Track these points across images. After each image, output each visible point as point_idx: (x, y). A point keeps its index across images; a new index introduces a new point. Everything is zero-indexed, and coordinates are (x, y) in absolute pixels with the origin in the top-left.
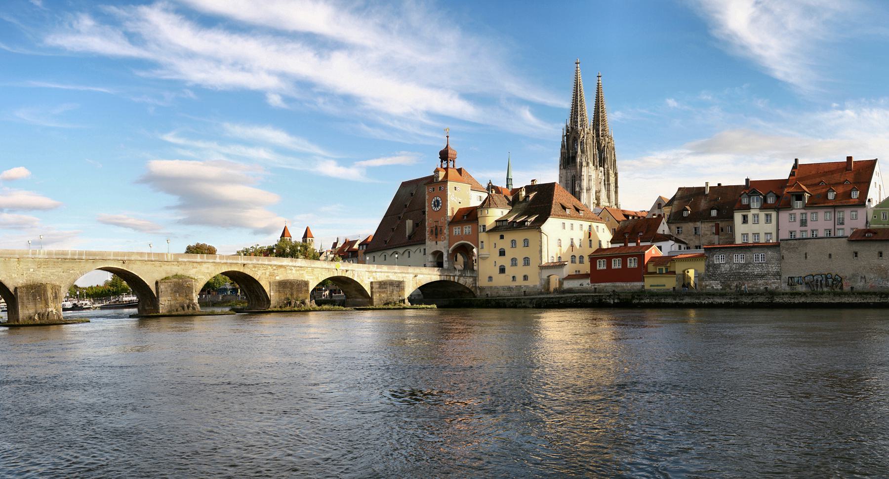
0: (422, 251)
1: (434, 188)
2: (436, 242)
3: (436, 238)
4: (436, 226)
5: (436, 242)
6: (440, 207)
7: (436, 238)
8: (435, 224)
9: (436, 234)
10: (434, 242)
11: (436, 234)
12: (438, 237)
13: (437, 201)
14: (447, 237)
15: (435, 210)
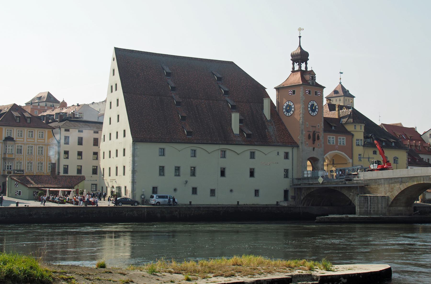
0: (282, 155)
1: (309, 91)
2: (314, 148)
3: (314, 143)
4: (314, 132)
5: (314, 148)
6: (316, 113)
7: (314, 143)
8: (312, 130)
9: (314, 140)
10: (311, 148)
11: (314, 140)
12: (316, 142)
13: (313, 105)
14: (323, 145)
15: (314, 115)
